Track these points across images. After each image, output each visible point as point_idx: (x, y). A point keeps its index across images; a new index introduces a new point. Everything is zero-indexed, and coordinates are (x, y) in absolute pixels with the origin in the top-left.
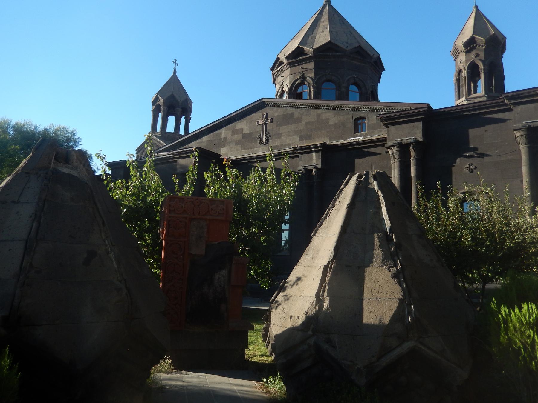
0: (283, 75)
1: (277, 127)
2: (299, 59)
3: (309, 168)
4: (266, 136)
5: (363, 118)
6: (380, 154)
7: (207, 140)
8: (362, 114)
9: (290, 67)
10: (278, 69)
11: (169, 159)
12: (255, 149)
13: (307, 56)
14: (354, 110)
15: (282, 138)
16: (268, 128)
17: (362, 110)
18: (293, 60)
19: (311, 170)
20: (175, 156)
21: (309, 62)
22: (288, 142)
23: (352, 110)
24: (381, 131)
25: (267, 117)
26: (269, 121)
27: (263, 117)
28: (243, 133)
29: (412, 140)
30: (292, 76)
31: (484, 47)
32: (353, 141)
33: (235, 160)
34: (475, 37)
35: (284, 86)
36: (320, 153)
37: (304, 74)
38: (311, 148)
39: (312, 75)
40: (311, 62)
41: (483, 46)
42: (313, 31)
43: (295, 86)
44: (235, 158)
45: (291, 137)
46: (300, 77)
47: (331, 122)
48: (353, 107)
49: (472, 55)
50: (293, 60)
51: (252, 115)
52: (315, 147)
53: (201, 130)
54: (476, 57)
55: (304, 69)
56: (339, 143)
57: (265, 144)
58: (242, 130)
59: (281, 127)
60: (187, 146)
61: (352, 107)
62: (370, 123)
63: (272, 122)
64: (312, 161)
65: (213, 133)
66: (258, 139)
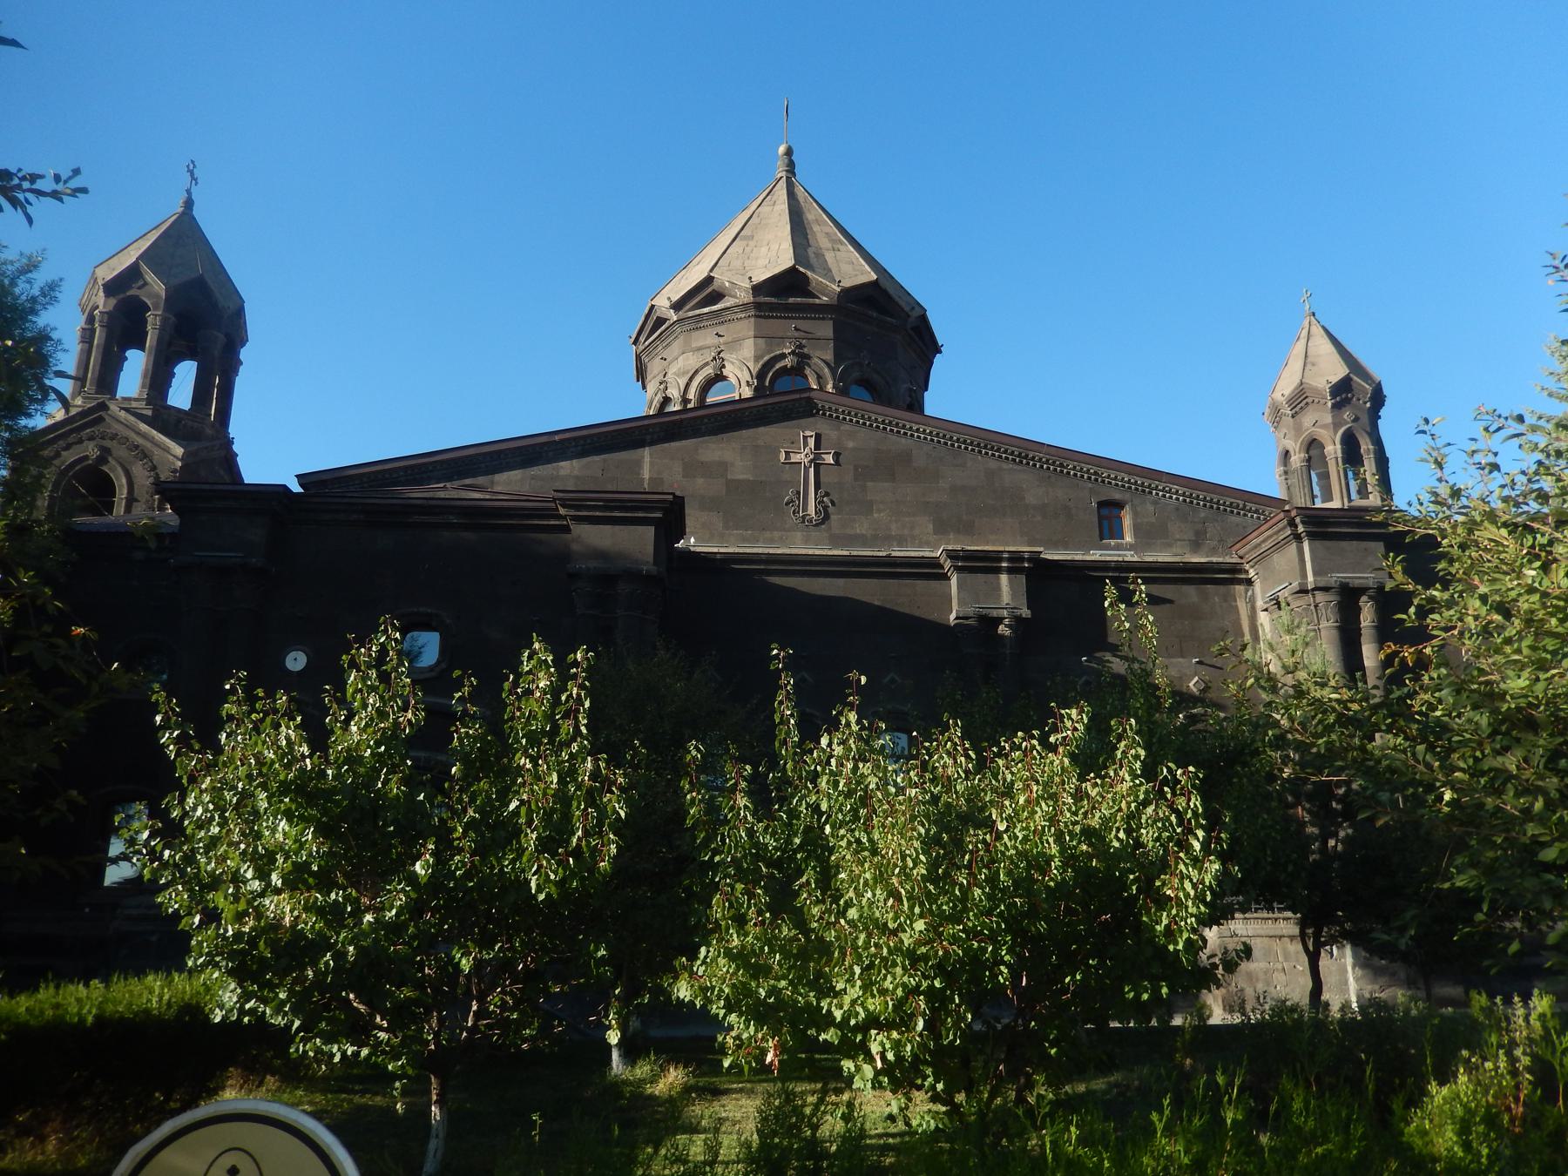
0: (720, 329)
1: (856, 479)
2: (791, 300)
3: (995, 613)
4: (819, 502)
5: (1119, 505)
6: (1170, 602)
7: (576, 472)
8: (1117, 496)
9: (756, 316)
10: (706, 310)
11: (511, 517)
12: (776, 534)
13: (817, 301)
14: (1096, 480)
15: (876, 515)
16: (823, 479)
17: (1117, 485)
18: (773, 300)
19: (1000, 620)
20: (562, 511)
21: (819, 319)
22: (894, 529)
23: (1089, 478)
24: (1170, 545)
25: (818, 445)
26: (829, 459)
27: (806, 443)
28: (729, 477)
29: (1371, 583)
30: (761, 341)
31: (1368, 405)
32: (1108, 559)
33: (712, 556)
34: (1351, 379)
35: (725, 363)
36: (1022, 579)
37: (801, 346)
38: (1001, 560)
39: (829, 356)
40: (823, 319)
41: (1365, 403)
42: (805, 236)
43: (774, 369)
44: (715, 550)
45: (907, 519)
46: (793, 353)
47: (1031, 499)
48: (1096, 473)
49: (1347, 415)
50: (773, 300)
51: (762, 429)
52: (1016, 558)
53: (557, 438)
54: (1353, 421)
55: (802, 334)
56: (1069, 558)
57: (816, 525)
58: (724, 466)
59: (870, 484)
60: (480, 480)
61: (1092, 471)
62: (1139, 521)
63: (837, 463)
64: (999, 596)
65: (603, 456)
66: (787, 504)
